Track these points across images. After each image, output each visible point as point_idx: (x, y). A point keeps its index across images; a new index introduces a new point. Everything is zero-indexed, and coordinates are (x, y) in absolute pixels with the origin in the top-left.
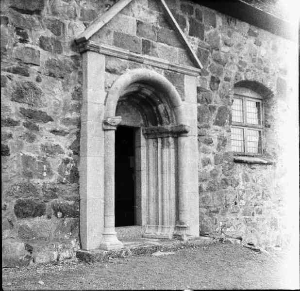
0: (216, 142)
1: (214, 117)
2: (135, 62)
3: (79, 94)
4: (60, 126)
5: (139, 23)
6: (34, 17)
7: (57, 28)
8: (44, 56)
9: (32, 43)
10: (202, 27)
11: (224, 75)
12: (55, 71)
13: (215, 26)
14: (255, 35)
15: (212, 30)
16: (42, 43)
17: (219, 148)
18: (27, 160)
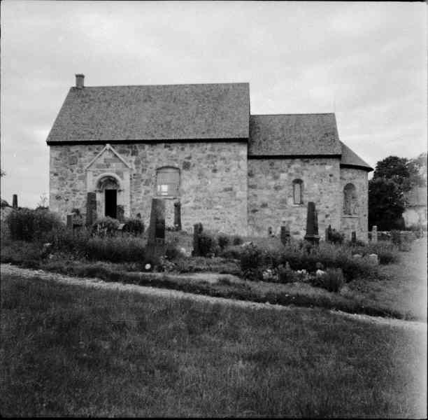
0: (143, 192)
1: (143, 183)
2: (104, 171)
3: (86, 184)
4: (82, 192)
5: (105, 159)
6: (75, 165)
7: (81, 166)
8: (78, 175)
9: (74, 172)
10: (137, 152)
11: (149, 166)
12: (80, 178)
13: (144, 148)
14: (169, 147)
15: (143, 151)
16: (78, 172)
17: (145, 194)
18: (74, 202)
